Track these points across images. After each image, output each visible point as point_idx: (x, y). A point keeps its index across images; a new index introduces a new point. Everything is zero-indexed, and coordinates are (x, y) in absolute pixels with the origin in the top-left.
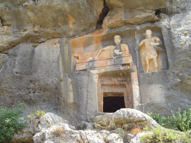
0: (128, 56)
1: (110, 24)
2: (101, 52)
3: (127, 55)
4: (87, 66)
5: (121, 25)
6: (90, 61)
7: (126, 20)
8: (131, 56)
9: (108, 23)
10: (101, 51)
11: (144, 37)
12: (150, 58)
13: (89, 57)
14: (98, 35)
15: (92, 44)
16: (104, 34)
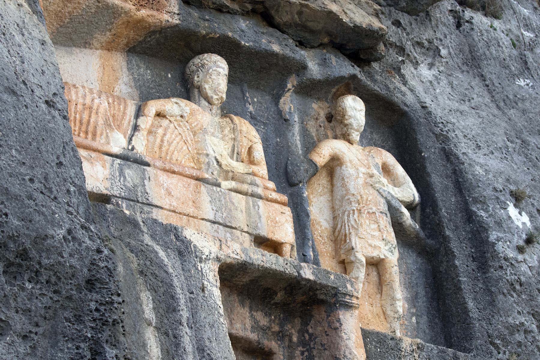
0: (276, 201)
11: (336, 123)
12: (375, 254)
15: (86, 44)
16: (170, 20)
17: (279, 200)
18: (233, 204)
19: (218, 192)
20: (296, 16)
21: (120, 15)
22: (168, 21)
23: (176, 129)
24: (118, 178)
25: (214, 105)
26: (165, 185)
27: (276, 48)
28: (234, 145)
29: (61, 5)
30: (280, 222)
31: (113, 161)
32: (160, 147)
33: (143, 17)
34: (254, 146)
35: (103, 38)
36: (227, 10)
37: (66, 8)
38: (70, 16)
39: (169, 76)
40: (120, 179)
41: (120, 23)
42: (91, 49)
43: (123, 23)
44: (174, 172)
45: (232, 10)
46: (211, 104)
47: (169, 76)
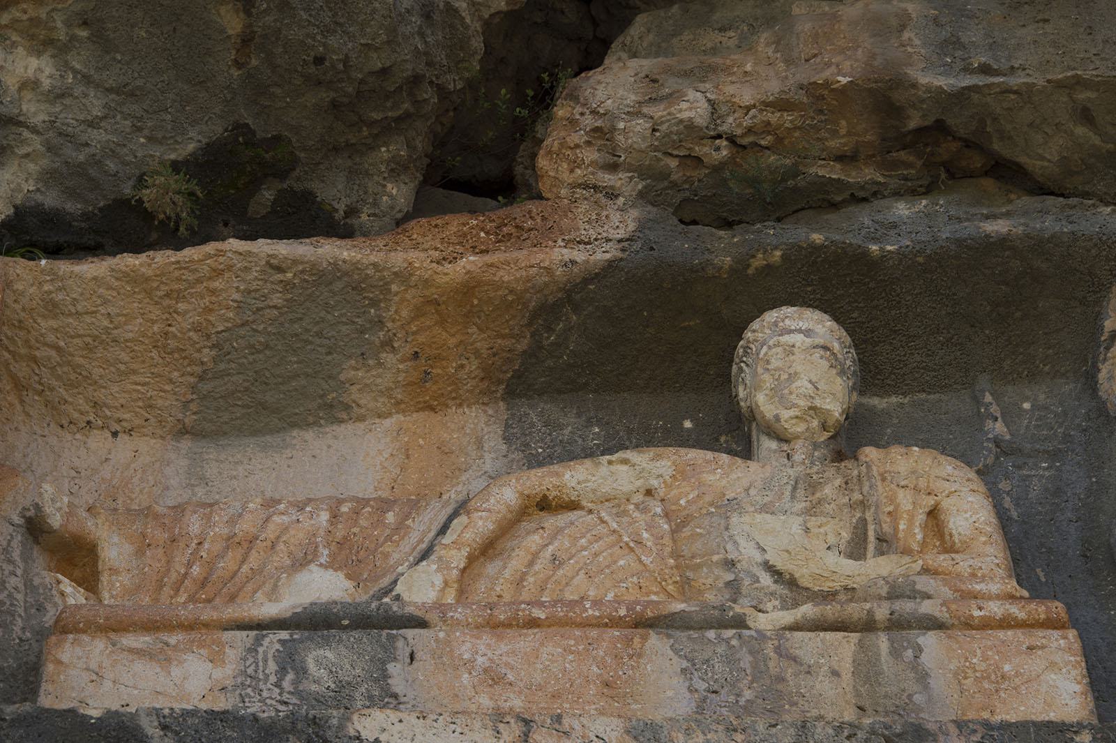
0: (1006, 623)
1: (690, 126)
2: (509, 527)
3: (996, 609)
4: (249, 680)
5: (868, 174)
6: (317, 622)
7: (962, 95)
8: (1050, 624)
9: (658, 111)
10: (507, 495)
13: (301, 562)
14: (471, 262)
15: (334, 411)
16: (579, 255)
17: (1022, 615)
18: (795, 659)
19: (727, 641)
20: (1080, 130)
21: (385, 289)
22: (573, 262)
23: (603, 522)
24: (273, 679)
25: (797, 437)
26: (480, 660)
27: (998, 227)
28: (863, 521)
29: (156, 312)
30: (1017, 674)
31: (258, 641)
32: (519, 582)
33: (468, 272)
34: (945, 504)
35: (379, 376)
36: (846, 195)
37: (179, 319)
38: (208, 337)
39: (688, 424)
40: (280, 680)
41: (405, 313)
42: (361, 419)
43: (418, 313)
44: (533, 623)
45: (862, 188)
46: (787, 441)
47: (688, 424)
